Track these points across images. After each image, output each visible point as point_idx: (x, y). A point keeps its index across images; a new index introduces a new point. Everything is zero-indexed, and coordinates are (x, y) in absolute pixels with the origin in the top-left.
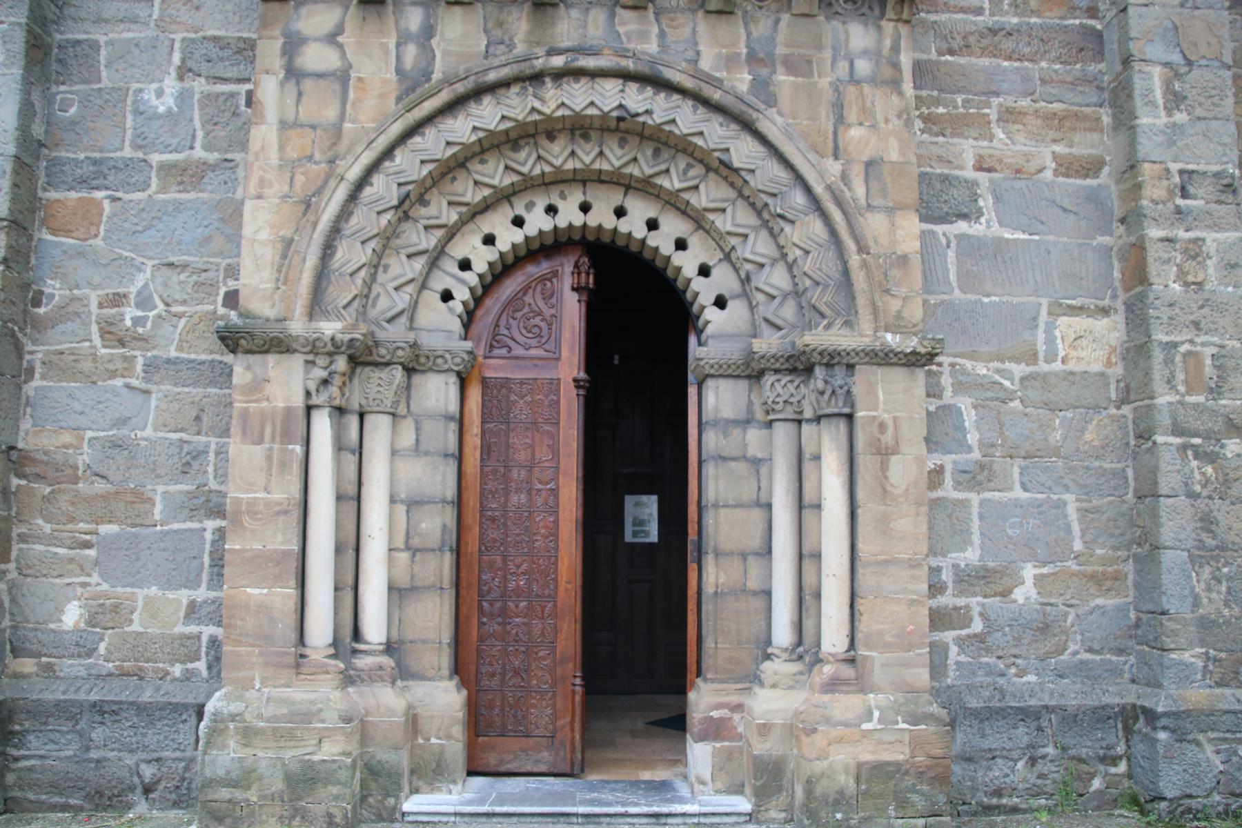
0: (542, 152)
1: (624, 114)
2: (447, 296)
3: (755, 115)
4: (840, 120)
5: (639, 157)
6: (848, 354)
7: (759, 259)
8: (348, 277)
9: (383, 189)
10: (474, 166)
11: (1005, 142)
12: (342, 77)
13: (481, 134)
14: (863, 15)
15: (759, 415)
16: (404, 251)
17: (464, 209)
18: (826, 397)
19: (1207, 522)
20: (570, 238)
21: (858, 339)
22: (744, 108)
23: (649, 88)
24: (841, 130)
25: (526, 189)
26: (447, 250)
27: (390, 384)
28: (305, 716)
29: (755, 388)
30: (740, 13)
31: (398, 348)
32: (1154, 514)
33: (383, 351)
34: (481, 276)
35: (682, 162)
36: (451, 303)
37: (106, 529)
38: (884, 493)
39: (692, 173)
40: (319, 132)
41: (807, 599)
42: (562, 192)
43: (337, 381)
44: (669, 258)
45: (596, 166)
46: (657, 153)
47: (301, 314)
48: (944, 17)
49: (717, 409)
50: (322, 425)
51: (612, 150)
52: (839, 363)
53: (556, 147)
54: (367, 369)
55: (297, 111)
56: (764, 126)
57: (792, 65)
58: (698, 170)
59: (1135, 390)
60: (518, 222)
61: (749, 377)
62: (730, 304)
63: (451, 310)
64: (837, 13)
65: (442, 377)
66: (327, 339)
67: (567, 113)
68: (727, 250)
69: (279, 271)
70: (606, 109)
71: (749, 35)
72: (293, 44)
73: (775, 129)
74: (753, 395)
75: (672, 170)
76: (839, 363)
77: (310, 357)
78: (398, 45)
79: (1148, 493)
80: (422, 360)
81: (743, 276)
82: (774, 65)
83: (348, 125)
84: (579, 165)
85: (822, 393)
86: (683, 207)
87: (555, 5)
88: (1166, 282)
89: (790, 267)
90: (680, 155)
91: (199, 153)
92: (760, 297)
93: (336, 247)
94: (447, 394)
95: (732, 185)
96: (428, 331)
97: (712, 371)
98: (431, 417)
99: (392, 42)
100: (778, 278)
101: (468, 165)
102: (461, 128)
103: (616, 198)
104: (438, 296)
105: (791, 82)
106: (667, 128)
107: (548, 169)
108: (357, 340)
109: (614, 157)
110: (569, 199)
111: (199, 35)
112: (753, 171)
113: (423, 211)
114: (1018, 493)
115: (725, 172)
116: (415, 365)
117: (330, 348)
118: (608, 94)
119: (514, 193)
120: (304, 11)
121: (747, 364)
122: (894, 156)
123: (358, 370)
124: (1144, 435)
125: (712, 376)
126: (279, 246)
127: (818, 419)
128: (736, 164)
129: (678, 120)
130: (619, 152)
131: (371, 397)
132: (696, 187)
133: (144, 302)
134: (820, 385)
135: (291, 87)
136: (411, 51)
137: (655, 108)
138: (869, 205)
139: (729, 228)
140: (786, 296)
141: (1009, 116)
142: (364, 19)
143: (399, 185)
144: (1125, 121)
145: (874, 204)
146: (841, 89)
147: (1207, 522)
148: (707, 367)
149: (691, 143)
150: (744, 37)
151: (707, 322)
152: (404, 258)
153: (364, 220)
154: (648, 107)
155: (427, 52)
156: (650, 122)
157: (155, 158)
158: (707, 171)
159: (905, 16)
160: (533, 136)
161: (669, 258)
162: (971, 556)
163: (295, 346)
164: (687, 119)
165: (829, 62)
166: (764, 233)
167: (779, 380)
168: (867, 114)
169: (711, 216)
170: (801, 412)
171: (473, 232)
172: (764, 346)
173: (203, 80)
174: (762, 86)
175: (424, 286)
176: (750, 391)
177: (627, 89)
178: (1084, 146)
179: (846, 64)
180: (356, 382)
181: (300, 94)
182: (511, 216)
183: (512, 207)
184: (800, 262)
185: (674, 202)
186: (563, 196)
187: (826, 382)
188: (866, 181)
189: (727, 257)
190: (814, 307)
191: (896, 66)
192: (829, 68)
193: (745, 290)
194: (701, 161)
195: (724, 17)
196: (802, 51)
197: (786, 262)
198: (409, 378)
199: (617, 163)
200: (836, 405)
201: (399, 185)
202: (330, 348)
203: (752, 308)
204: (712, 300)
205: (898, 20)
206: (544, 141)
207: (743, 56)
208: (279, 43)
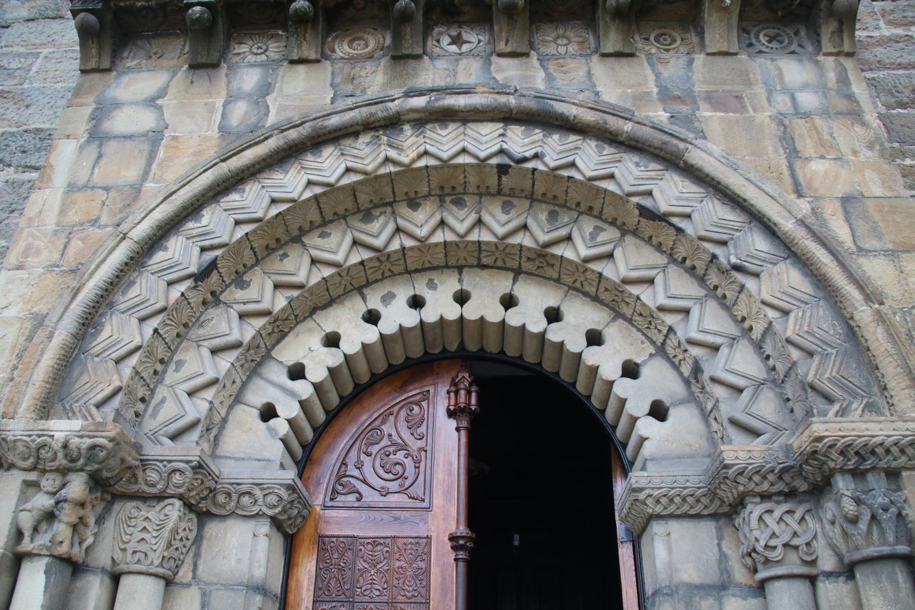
0: (401, 222)
1: (506, 161)
2: (268, 413)
3: (682, 145)
4: (793, 154)
5: (531, 223)
6: (888, 451)
7: (711, 339)
8: (111, 364)
9: (182, 253)
10: (313, 240)
12: (154, 138)
13: (318, 190)
14: (793, 53)
15: (740, 575)
16: (206, 343)
17: (295, 293)
18: (863, 526)
20: (444, 350)
21: (900, 424)
22: (666, 138)
23: (537, 131)
24: (798, 165)
25: (384, 278)
26: (274, 353)
27: (160, 527)
29: (728, 532)
30: (643, 56)
31: (174, 471)
33: (153, 476)
34: (317, 387)
35: (588, 225)
36: (273, 422)
39: (602, 237)
40: (112, 194)
42: (431, 280)
43: (68, 514)
44: (580, 355)
45: (474, 237)
46: (553, 216)
47: (28, 409)
48: (882, 74)
49: (670, 567)
51: (493, 216)
52: (873, 468)
53: (420, 216)
54: (130, 505)
55: (92, 173)
56: (695, 157)
57: (715, 101)
58: (610, 234)
60: (372, 318)
61: (714, 516)
62: (673, 413)
63: (272, 431)
64: (760, 52)
65: (250, 525)
66: (57, 445)
67: (432, 162)
68: (659, 339)
69: (20, 357)
70: (482, 155)
71: (658, 76)
73: (711, 159)
74: (724, 545)
75: (576, 236)
76: (873, 468)
77: (33, 476)
78: (225, 105)
80: (221, 498)
81: (686, 370)
82: (694, 102)
83: (149, 185)
84: (450, 237)
85: (854, 521)
86: (592, 291)
87: (418, 57)
89: (758, 346)
90: (584, 218)
92: (719, 392)
93: (102, 325)
94: (253, 552)
95: (659, 247)
96: (237, 459)
97: (658, 509)
98: (228, 586)
99: (219, 102)
100: (742, 362)
101: (304, 239)
103: (503, 284)
104: (256, 413)
105: (721, 118)
106: (565, 173)
107: (409, 243)
108: (102, 447)
110: (440, 288)
111: (21, 129)
112: (688, 216)
113: (240, 294)
115: (648, 227)
116: (205, 503)
117: (61, 461)
118: (484, 139)
119: (368, 284)
120: (125, 79)
121: (712, 494)
122: (878, 191)
123: (116, 507)
125: (659, 517)
126: (28, 325)
127: (848, 571)
128: (664, 207)
129: (579, 162)
130: (504, 218)
131: (130, 548)
132: (610, 256)
134: (849, 507)
135: (92, 152)
137: (547, 150)
138: (860, 249)
139: (662, 300)
140: (759, 385)
142: (192, 82)
143: (203, 249)
145: (867, 246)
146: (786, 122)
148: (649, 501)
149: (598, 189)
150: (651, 78)
151: (643, 440)
152: (206, 353)
153: (148, 289)
154: (539, 150)
156: (541, 167)
158: (623, 235)
159: (846, 48)
160: (391, 204)
161: (580, 355)
163: (11, 458)
164: (590, 159)
165: (764, 97)
166: (712, 306)
167: (770, 512)
169: (634, 290)
170: (813, 563)
171: (311, 331)
172: (741, 454)
173: (12, 169)
175: (238, 399)
176: (720, 538)
177: (509, 133)
179: (787, 99)
180: (110, 524)
181: (100, 156)
182: (363, 309)
183: (364, 299)
184: (777, 327)
186: (432, 285)
187: (858, 501)
188: (848, 220)
189: (661, 350)
190: (813, 387)
191: (850, 97)
192: (765, 102)
193: (692, 394)
194: (613, 223)
195: (624, 60)
196: (727, 88)
197: (751, 340)
198: (201, 526)
199: (501, 231)
200: (884, 542)
201: (203, 249)
202: (61, 461)
203: (705, 416)
204: (647, 409)
205: (838, 54)
206: (403, 209)
207: (655, 95)
208: (88, 111)
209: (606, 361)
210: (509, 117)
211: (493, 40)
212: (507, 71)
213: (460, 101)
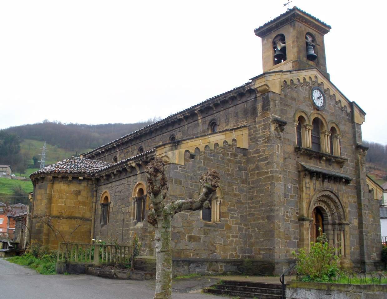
4: (343, 197)
19: (367, 242)
37: (288, 241)
38: (347, 239)
72: (306, 183)
100: (336, 214)
114: (352, 239)
155: (315, 186)
157: (290, 194)
174: (338, 192)
210: (329, 191)
211: (328, 181)
212: (329, 184)
213: (328, 190)
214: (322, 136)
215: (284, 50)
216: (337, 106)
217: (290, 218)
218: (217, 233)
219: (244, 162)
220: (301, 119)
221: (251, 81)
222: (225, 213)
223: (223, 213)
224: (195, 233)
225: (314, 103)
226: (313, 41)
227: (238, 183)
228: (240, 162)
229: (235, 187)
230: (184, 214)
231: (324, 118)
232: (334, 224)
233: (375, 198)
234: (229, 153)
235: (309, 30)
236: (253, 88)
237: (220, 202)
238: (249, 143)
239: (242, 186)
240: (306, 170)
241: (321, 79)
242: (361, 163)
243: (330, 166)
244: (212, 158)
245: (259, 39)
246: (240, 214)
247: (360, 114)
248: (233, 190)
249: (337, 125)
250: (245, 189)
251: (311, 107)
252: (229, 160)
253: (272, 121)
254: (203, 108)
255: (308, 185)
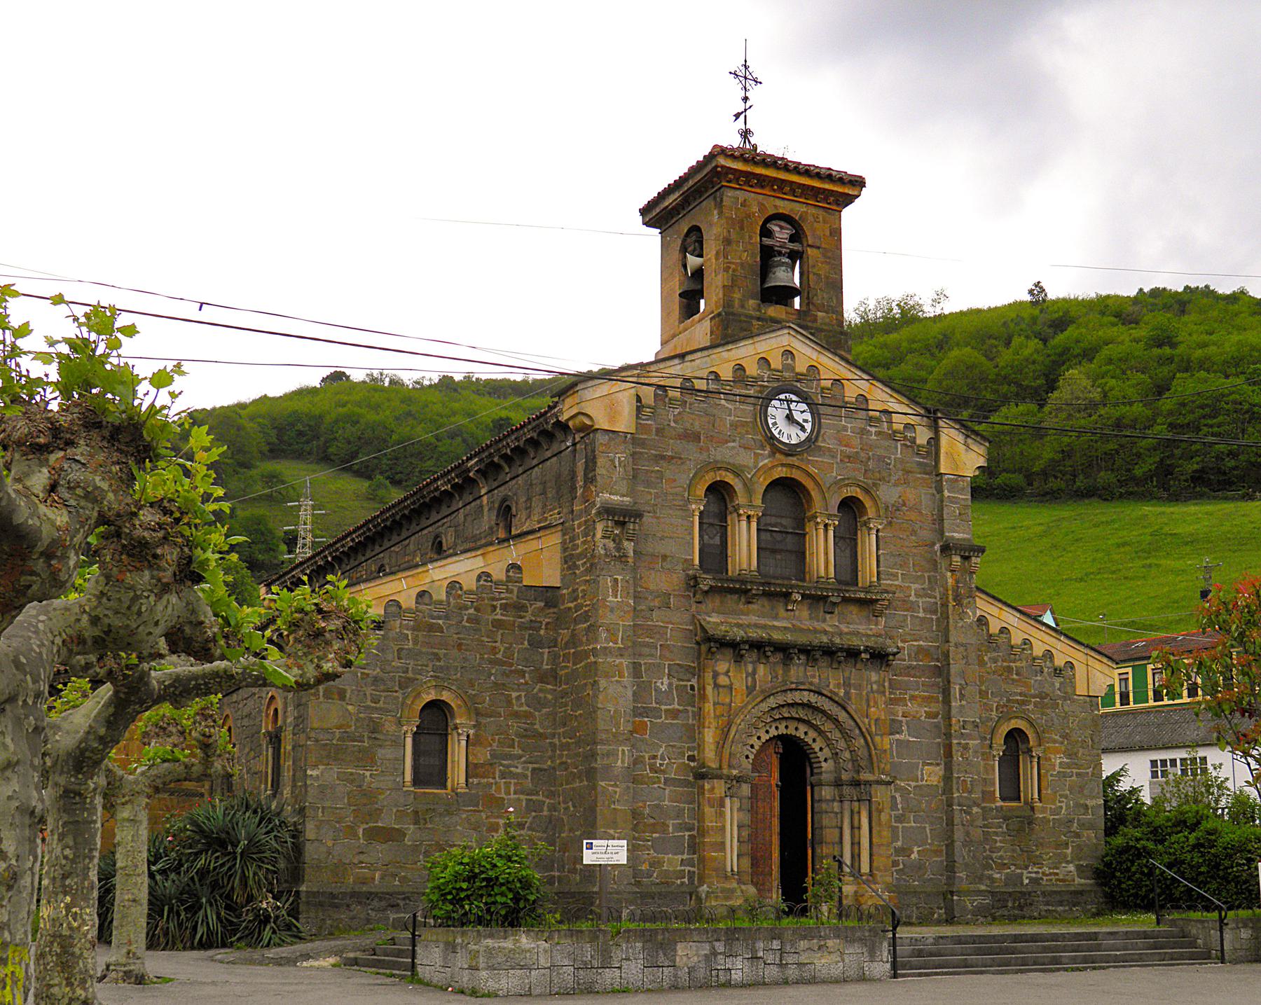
2: (747, 757)
4: (868, 706)
11: (911, 707)
19: (968, 833)
28: (733, 891)
32: (953, 832)
38: (880, 824)
41: (856, 857)
50: (728, 801)
59: (948, 790)
60: (767, 732)
79: (950, 823)
88: (957, 758)
91: (677, 707)
100: (847, 755)
102: (764, 707)
109: (802, 714)
124: (950, 805)
133: (663, 759)
136: (750, 679)
141: (913, 698)
144: (947, 702)
147: (968, 833)
155: (754, 681)
162: (899, 844)
168: (876, 703)
178: (935, 707)
185: (815, 728)
209: (816, 747)
212: (810, 671)
214: (809, 527)
215: (699, 274)
216: (873, 430)
217: (664, 772)
218: (455, 819)
219: (547, 624)
220: (720, 491)
221: (556, 399)
222: (482, 765)
223: (476, 765)
224: (387, 821)
225: (773, 437)
226: (792, 239)
227: (526, 683)
228: (534, 626)
229: (514, 695)
230: (352, 774)
231: (808, 474)
232: (838, 783)
233: (1081, 689)
234: (498, 603)
235: (775, 206)
236: (563, 418)
237: (468, 736)
238: (562, 570)
239: (540, 690)
240: (709, 639)
241: (807, 354)
242: (958, 598)
243: (828, 616)
244: (440, 622)
245: (653, 236)
246: (531, 766)
247: (966, 444)
248: (509, 702)
249: (867, 491)
250: (550, 697)
251: (763, 447)
252: (498, 624)
253: (599, 513)
254: (482, 466)
255: (723, 680)
